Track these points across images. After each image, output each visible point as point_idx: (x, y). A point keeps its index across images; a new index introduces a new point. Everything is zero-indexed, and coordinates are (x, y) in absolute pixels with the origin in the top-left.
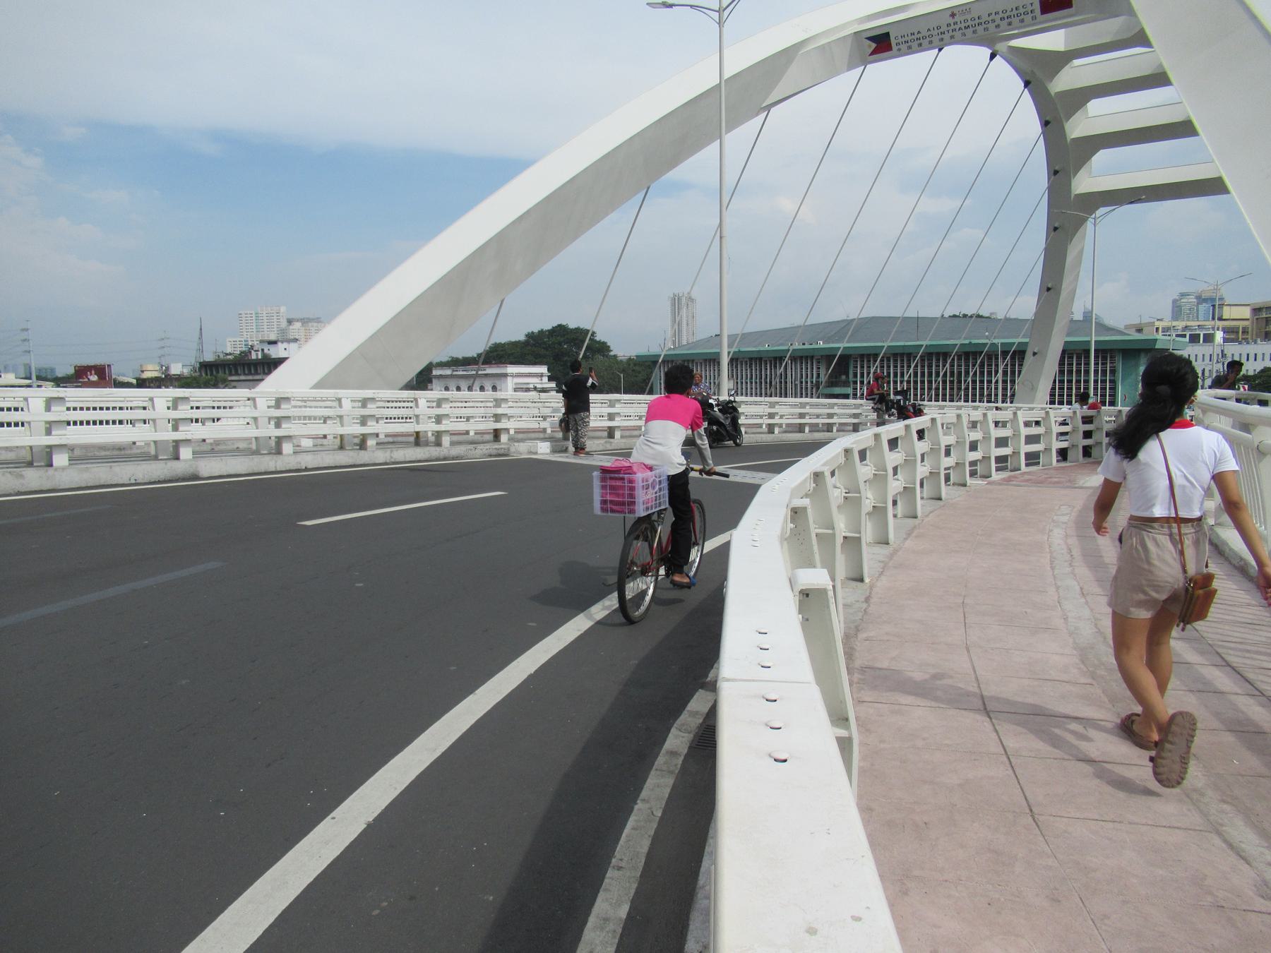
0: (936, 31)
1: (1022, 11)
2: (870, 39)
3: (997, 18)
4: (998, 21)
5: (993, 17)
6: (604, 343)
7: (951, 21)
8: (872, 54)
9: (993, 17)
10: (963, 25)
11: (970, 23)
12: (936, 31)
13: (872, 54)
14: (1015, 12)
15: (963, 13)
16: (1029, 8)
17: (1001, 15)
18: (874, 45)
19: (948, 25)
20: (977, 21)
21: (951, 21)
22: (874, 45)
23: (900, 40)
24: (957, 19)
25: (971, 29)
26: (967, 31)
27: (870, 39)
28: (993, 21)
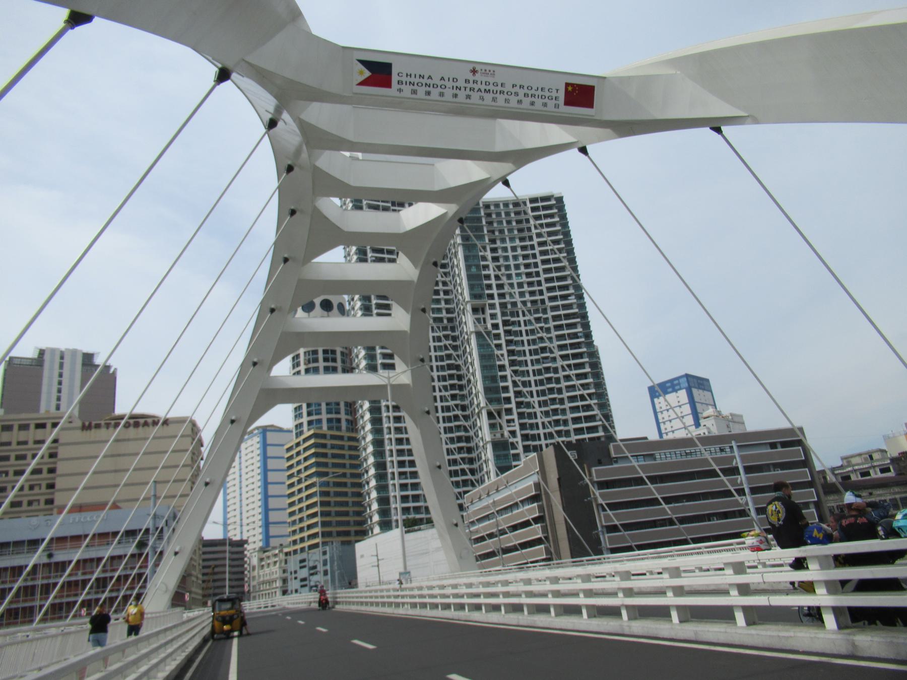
0: (450, 84)
1: (547, 94)
2: (364, 63)
3: (521, 92)
4: (521, 97)
5: (517, 89)
7: (471, 77)
8: (363, 83)
9: (517, 89)
10: (483, 87)
11: (491, 87)
12: (450, 84)
13: (363, 83)
14: (540, 92)
15: (485, 73)
16: (554, 94)
17: (526, 91)
18: (367, 74)
19: (467, 81)
20: (499, 88)
21: (471, 77)
22: (367, 74)
23: (404, 79)
24: (478, 77)
25: (491, 95)
26: (486, 95)
27: (362, 62)
28: (517, 94)
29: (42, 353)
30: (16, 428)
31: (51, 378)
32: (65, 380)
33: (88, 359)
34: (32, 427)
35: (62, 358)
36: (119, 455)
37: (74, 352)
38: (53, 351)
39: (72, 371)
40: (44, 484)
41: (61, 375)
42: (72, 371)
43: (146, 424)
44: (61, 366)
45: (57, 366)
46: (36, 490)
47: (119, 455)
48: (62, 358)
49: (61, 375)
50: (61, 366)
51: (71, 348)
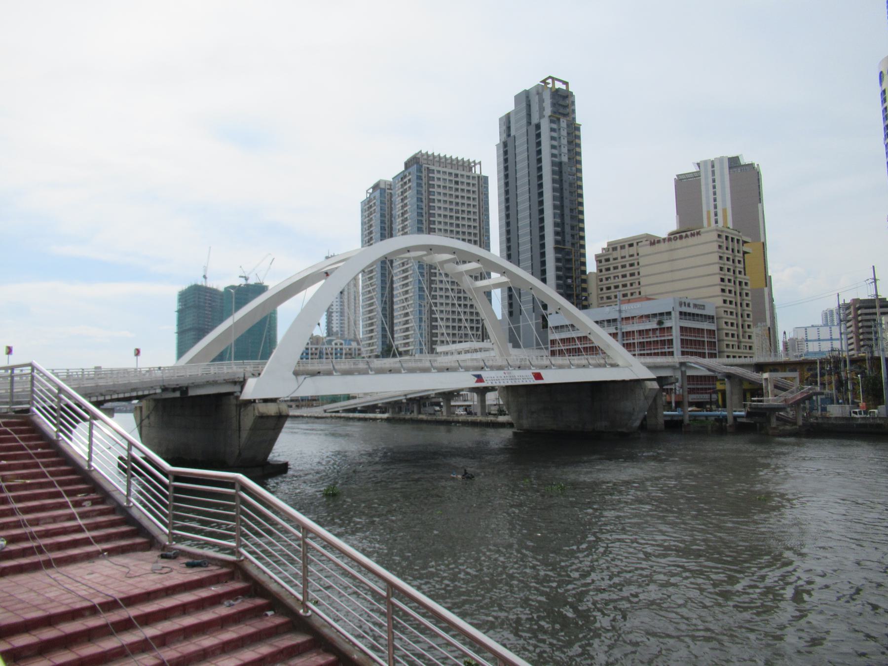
6: (517, 98)
29: (698, 164)
30: (619, 248)
31: (707, 184)
32: (717, 184)
33: (734, 162)
34: (627, 246)
35: (713, 166)
36: (673, 260)
37: (721, 159)
38: (705, 162)
39: (722, 175)
40: (637, 282)
41: (714, 181)
42: (722, 175)
43: (687, 236)
44: (713, 172)
45: (710, 173)
46: (634, 286)
47: (673, 260)
48: (713, 166)
49: (714, 181)
50: (713, 172)
51: (718, 156)
